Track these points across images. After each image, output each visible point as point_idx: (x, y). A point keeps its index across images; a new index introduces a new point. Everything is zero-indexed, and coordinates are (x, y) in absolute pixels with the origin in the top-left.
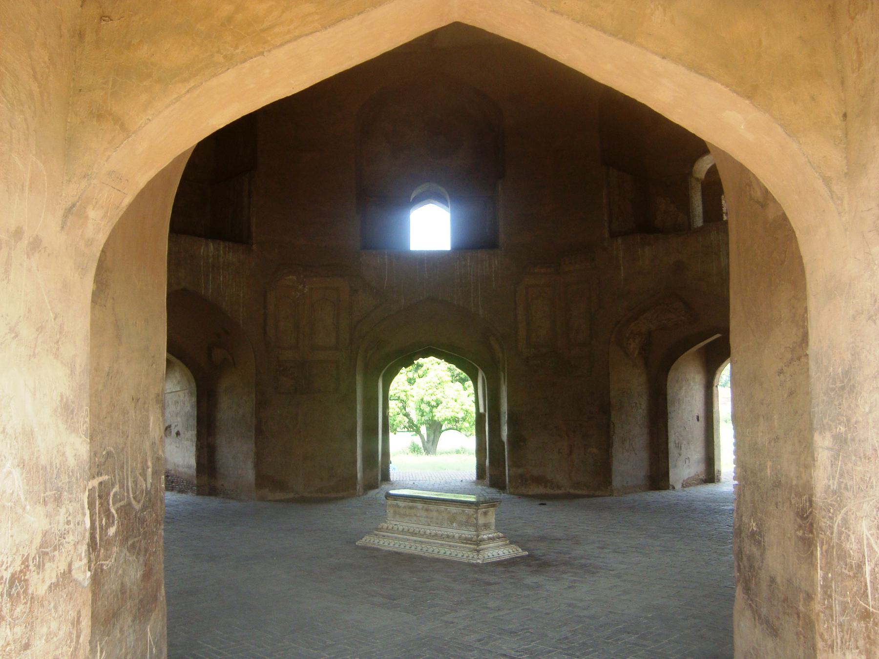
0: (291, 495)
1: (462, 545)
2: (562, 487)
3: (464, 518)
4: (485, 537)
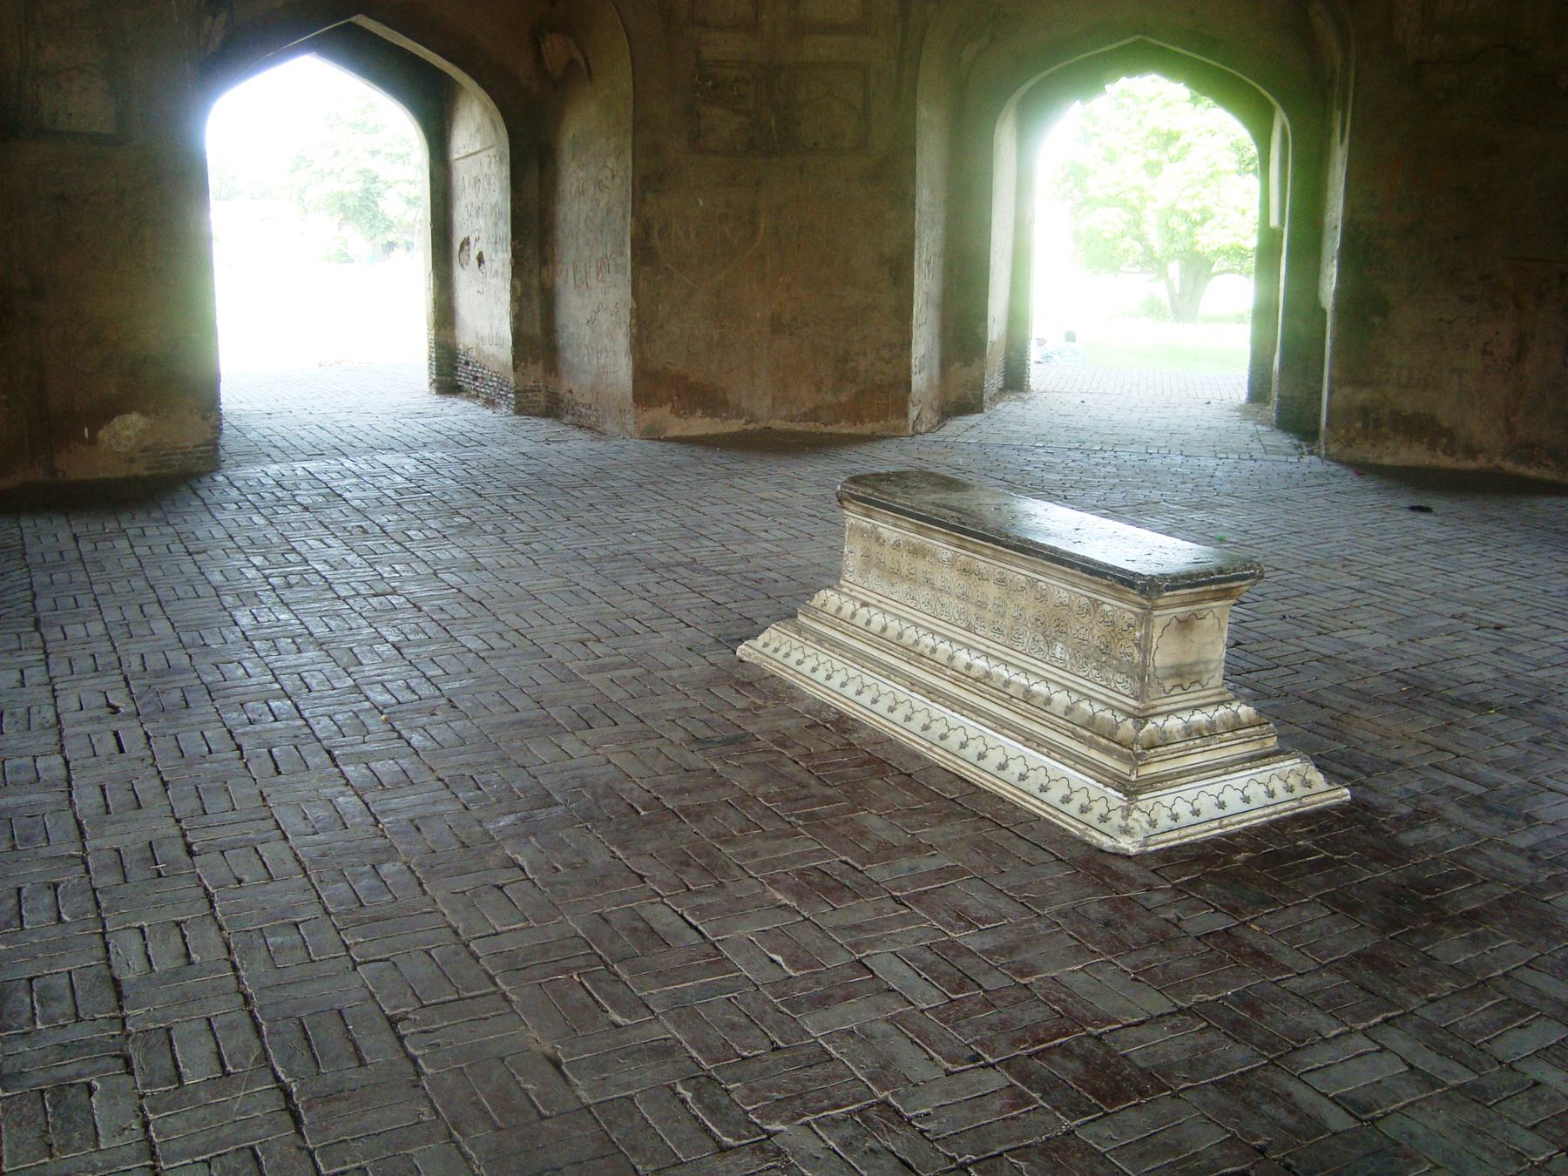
0: (735, 426)
1: (1073, 745)
2: (1481, 451)
3: (1095, 635)
4: (1174, 724)
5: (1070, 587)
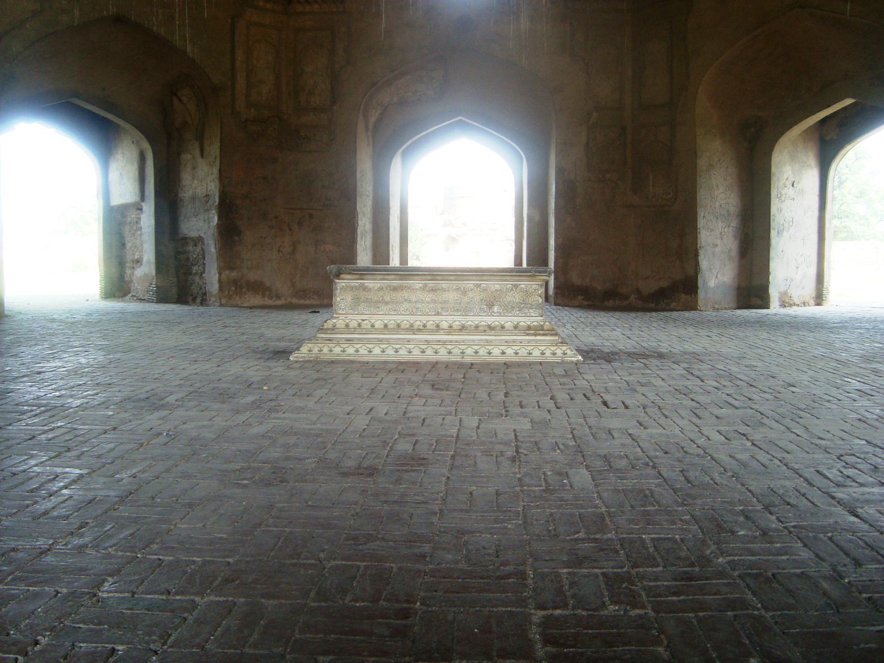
1: (527, 338)
3: (516, 297)
5: (500, 283)
